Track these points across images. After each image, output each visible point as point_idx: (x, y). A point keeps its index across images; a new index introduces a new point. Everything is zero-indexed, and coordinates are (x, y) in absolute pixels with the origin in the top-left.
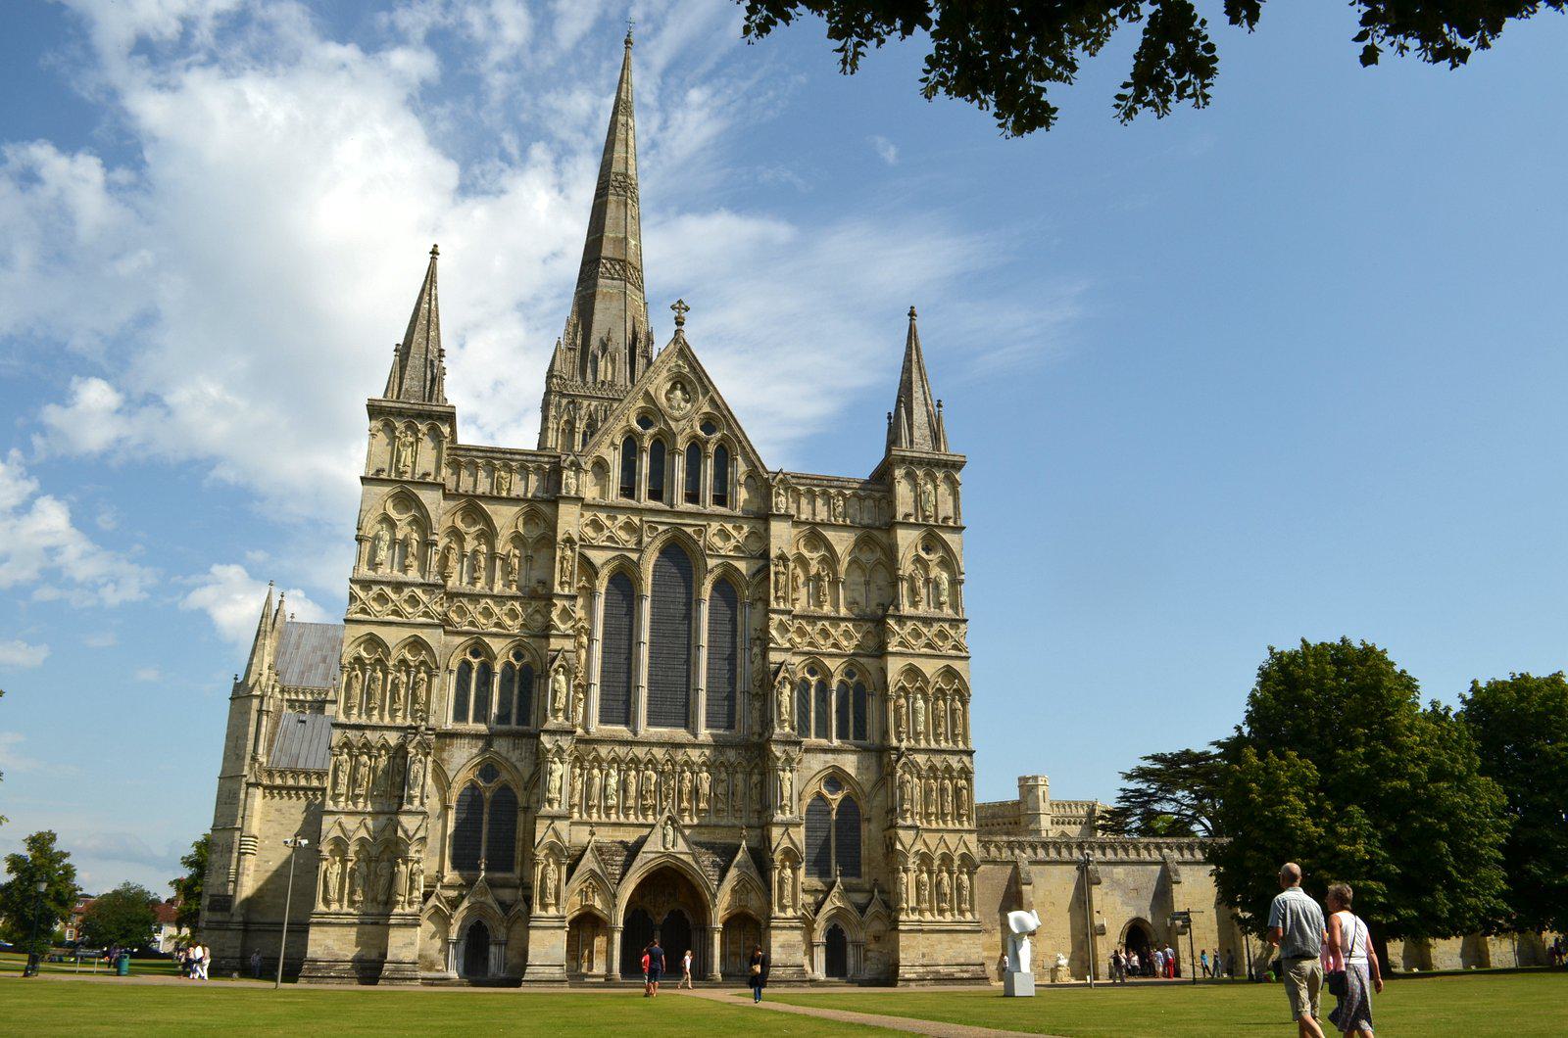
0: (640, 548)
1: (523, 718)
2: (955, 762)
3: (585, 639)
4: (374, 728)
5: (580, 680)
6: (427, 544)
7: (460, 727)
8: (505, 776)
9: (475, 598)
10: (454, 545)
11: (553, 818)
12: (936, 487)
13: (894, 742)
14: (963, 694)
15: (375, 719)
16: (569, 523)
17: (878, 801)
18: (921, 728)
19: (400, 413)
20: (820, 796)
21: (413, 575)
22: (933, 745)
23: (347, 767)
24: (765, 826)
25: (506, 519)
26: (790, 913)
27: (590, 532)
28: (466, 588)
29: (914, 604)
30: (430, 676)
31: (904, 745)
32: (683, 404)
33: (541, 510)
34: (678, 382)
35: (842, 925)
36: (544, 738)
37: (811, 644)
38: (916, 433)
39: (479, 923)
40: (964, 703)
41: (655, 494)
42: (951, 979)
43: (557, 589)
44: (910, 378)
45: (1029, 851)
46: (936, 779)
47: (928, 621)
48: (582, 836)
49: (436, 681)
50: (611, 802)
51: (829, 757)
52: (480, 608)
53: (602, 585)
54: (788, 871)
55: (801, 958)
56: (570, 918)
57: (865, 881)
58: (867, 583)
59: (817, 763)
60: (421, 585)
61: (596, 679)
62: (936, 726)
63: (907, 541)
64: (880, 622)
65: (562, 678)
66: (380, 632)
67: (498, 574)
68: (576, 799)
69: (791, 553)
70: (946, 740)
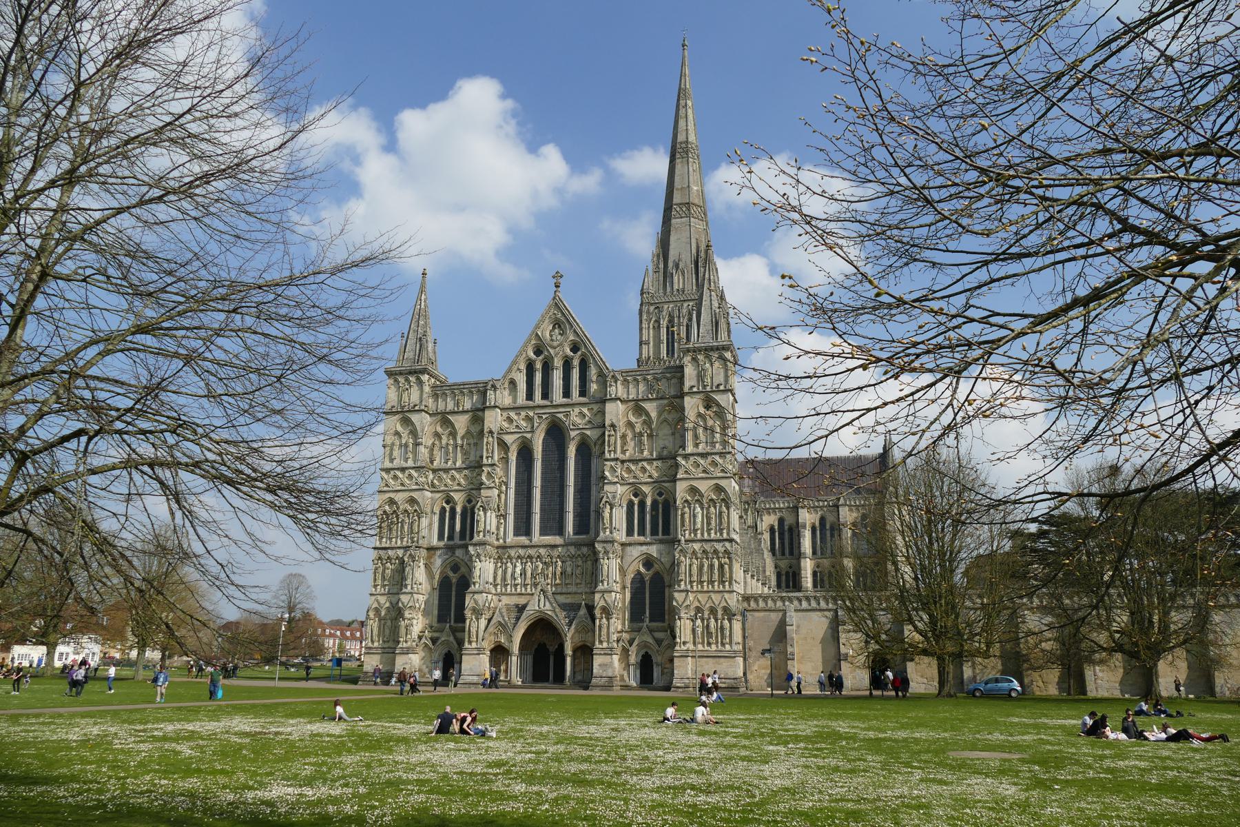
2: (719, 547)
3: (504, 488)
4: (392, 548)
10: (437, 442)
12: (712, 365)
16: (491, 422)
18: (699, 526)
19: (401, 373)
21: (410, 463)
23: (380, 570)
25: (461, 423)
27: (506, 425)
28: (443, 466)
29: (697, 445)
30: (419, 518)
32: (559, 337)
33: (477, 415)
36: (471, 548)
37: (635, 477)
41: (545, 395)
45: (796, 603)
46: (707, 559)
51: (644, 548)
53: (513, 456)
59: (635, 552)
60: (414, 468)
61: (511, 511)
62: (709, 524)
63: (692, 406)
65: (481, 513)
67: (459, 455)
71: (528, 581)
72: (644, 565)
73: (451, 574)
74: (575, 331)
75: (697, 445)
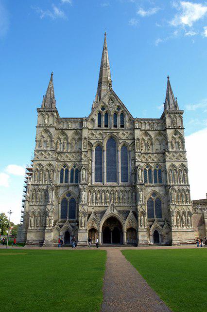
0: (103, 139)
1: (76, 182)
2: (185, 188)
5: (90, 171)
6: (52, 141)
7: (62, 184)
8: (72, 196)
9: (63, 153)
11: (83, 205)
13: (169, 183)
14: (186, 171)
15: (41, 183)
17: (166, 198)
20: (150, 198)
21: (48, 149)
22: (179, 184)
23: (35, 195)
24: (136, 206)
25: (70, 134)
26: (143, 227)
27: (90, 136)
29: (173, 148)
30: (53, 172)
31: (171, 184)
33: (78, 132)
34: (111, 99)
35: (157, 230)
36: (80, 186)
38: (171, 106)
39: (67, 231)
40: (187, 173)
41: (106, 126)
42: (186, 244)
43: (83, 150)
44: (168, 93)
47: (176, 152)
48: (91, 210)
49: (55, 174)
50: (98, 201)
51: (152, 188)
52: (65, 156)
53: (94, 148)
54: (142, 217)
55: (146, 239)
56: (88, 230)
57: (163, 219)
58: (160, 144)
61: (94, 171)
63: (169, 132)
64: (164, 153)
65: (84, 171)
66: (42, 162)
68: (90, 201)
69: (140, 138)
70: (183, 182)
71: (103, 201)
72: (152, 195)
73: (67, 197)
74: (119, 102)
75: (173, 148)
